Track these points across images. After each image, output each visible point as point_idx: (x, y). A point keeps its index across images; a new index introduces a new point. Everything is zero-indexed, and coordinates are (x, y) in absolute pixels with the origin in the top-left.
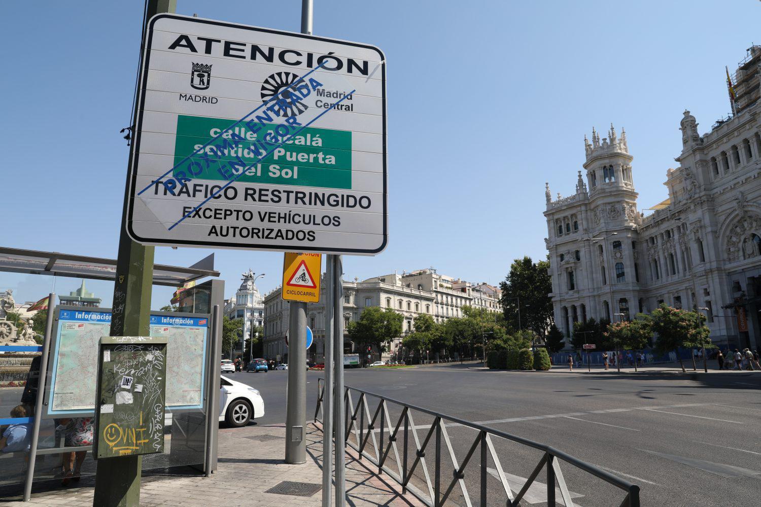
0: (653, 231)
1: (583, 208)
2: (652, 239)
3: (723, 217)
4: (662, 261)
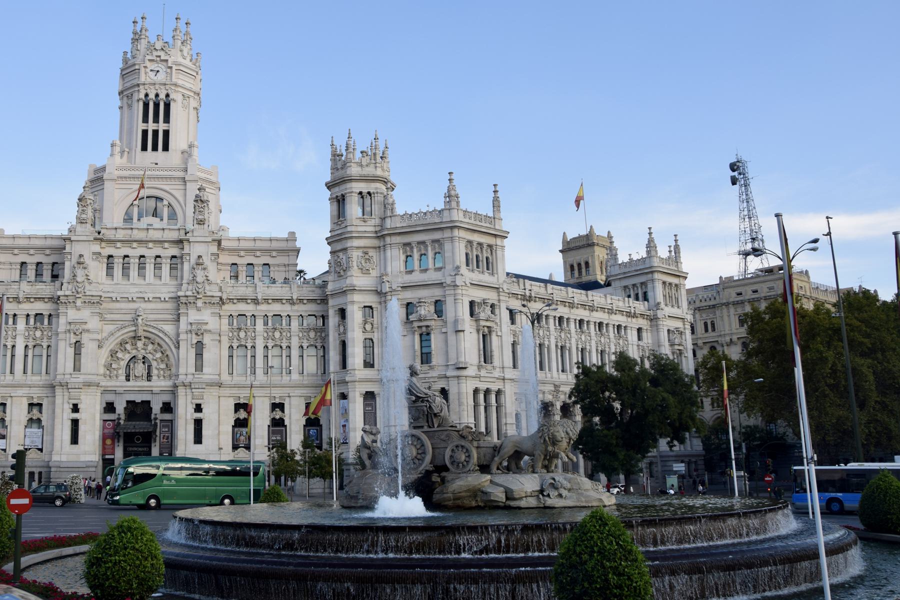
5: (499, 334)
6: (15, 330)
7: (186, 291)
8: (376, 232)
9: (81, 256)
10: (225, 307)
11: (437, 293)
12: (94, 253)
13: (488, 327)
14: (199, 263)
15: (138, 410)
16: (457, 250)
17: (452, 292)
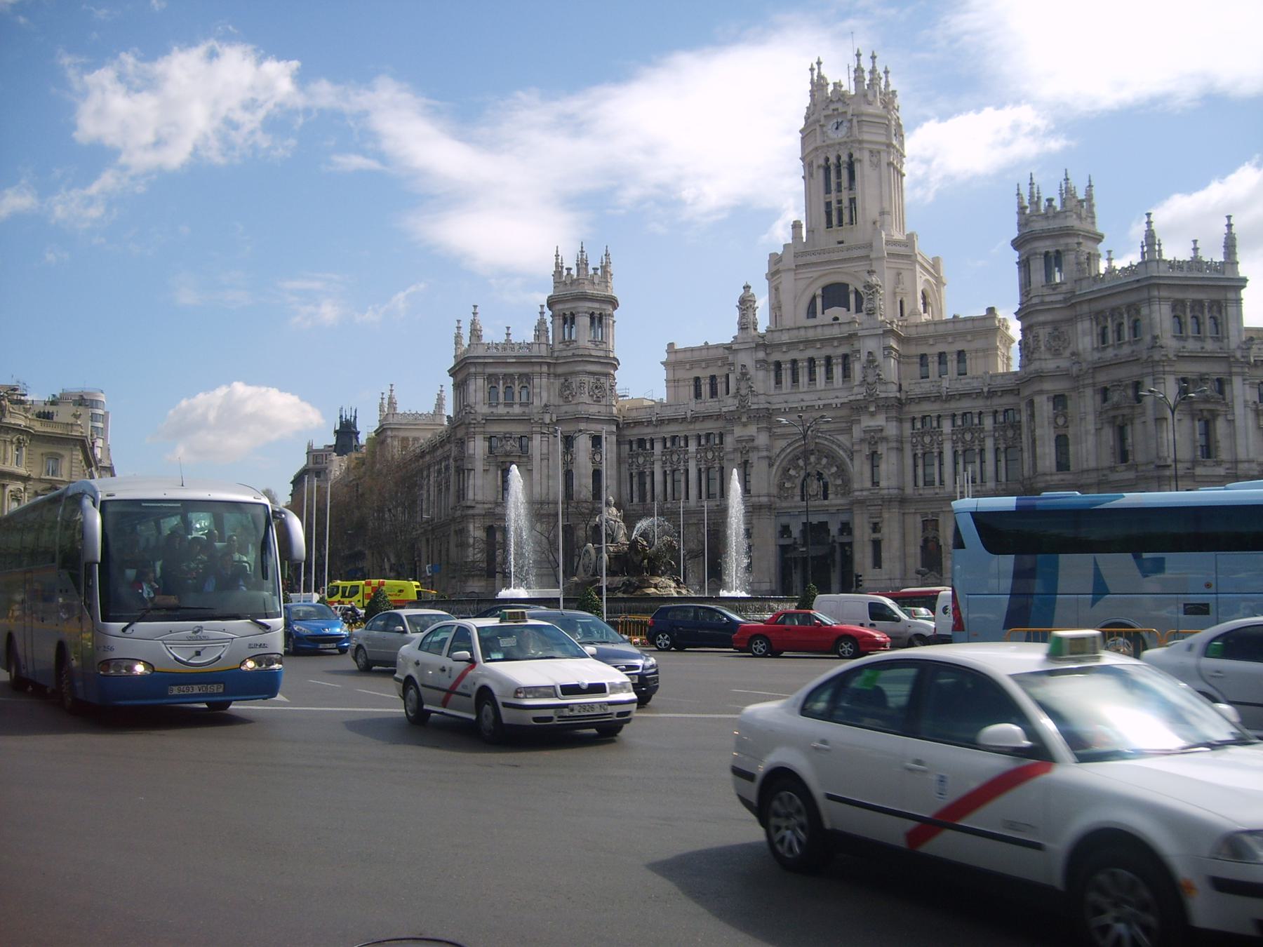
0: (646, 432)
1: (545, 369)
2: (641, 442)
3: (783, 443)
4: (658, 477)
5: (1230, 417)
6: (686, 452)
7: (859, 393)
8: (1065, 300)
9: (744, 366)
10: (906, 409)
11: (1135, 371)
12: (757, 362)
13: (1209, 410)
14: (871, 361)
15: (815, 531)
16: (1156, 316)
17: (1150, 370)
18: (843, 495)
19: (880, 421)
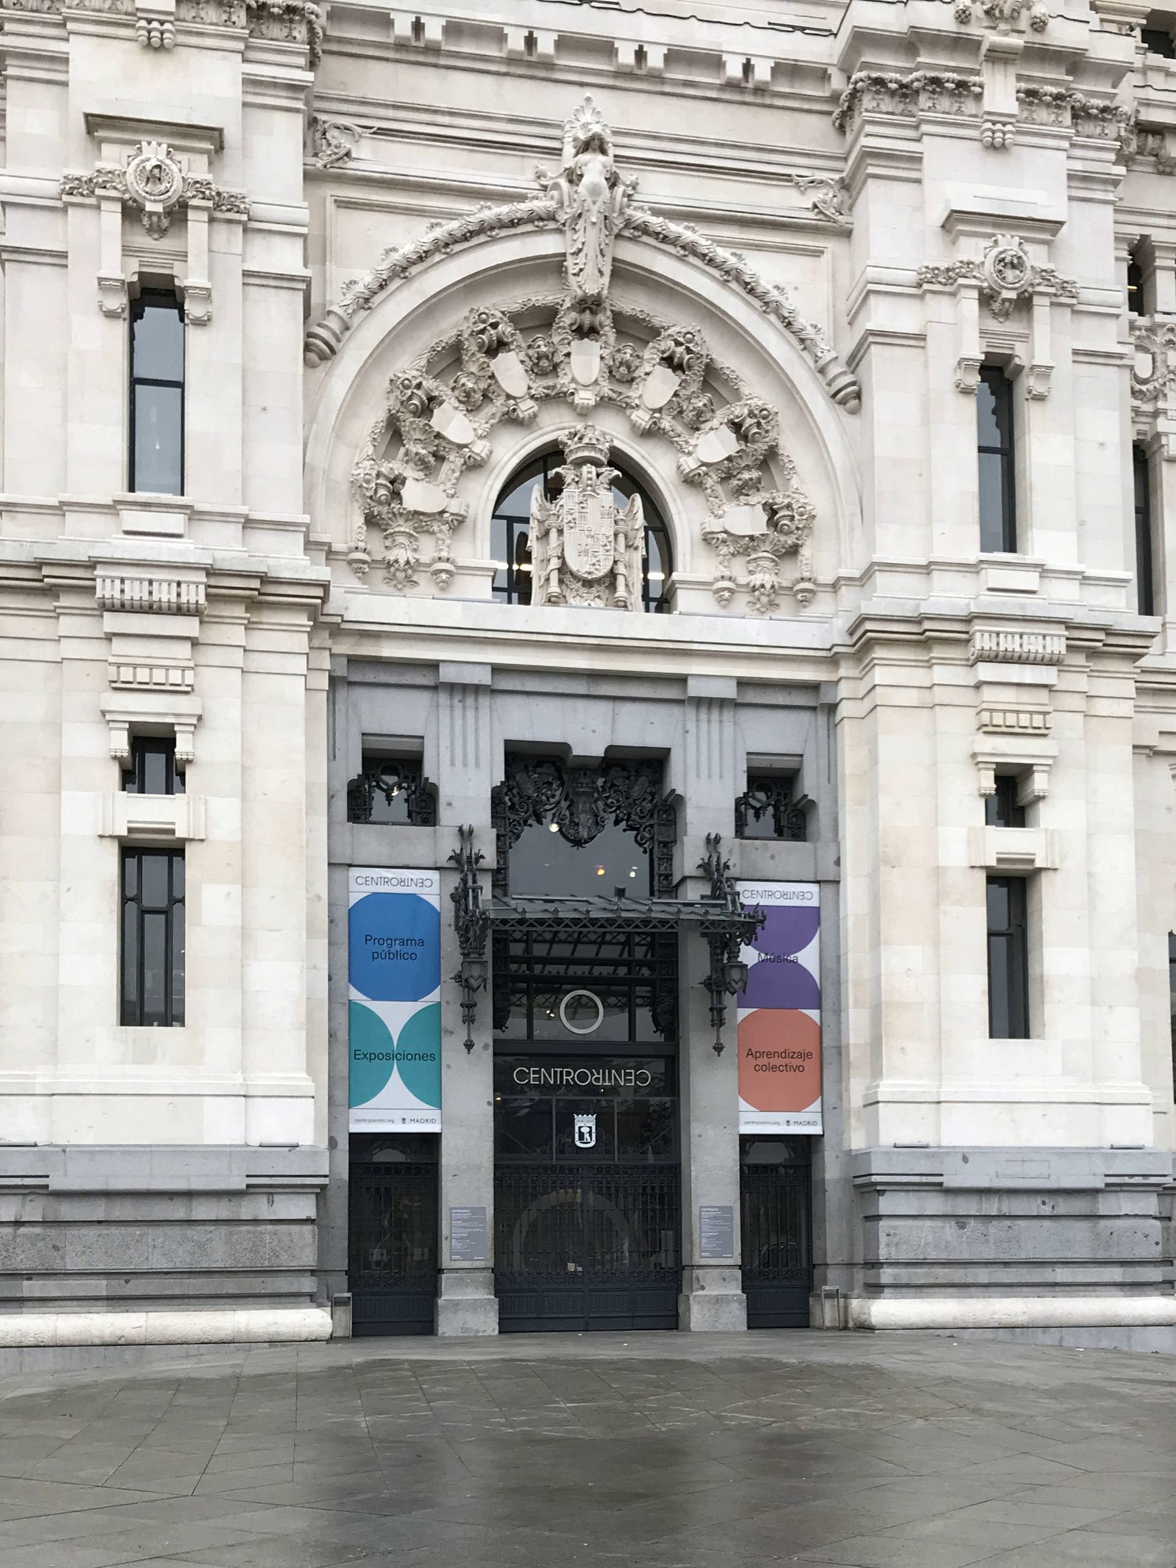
3: (410, 236)
18: (767, 600)
19: (1036, 180)
